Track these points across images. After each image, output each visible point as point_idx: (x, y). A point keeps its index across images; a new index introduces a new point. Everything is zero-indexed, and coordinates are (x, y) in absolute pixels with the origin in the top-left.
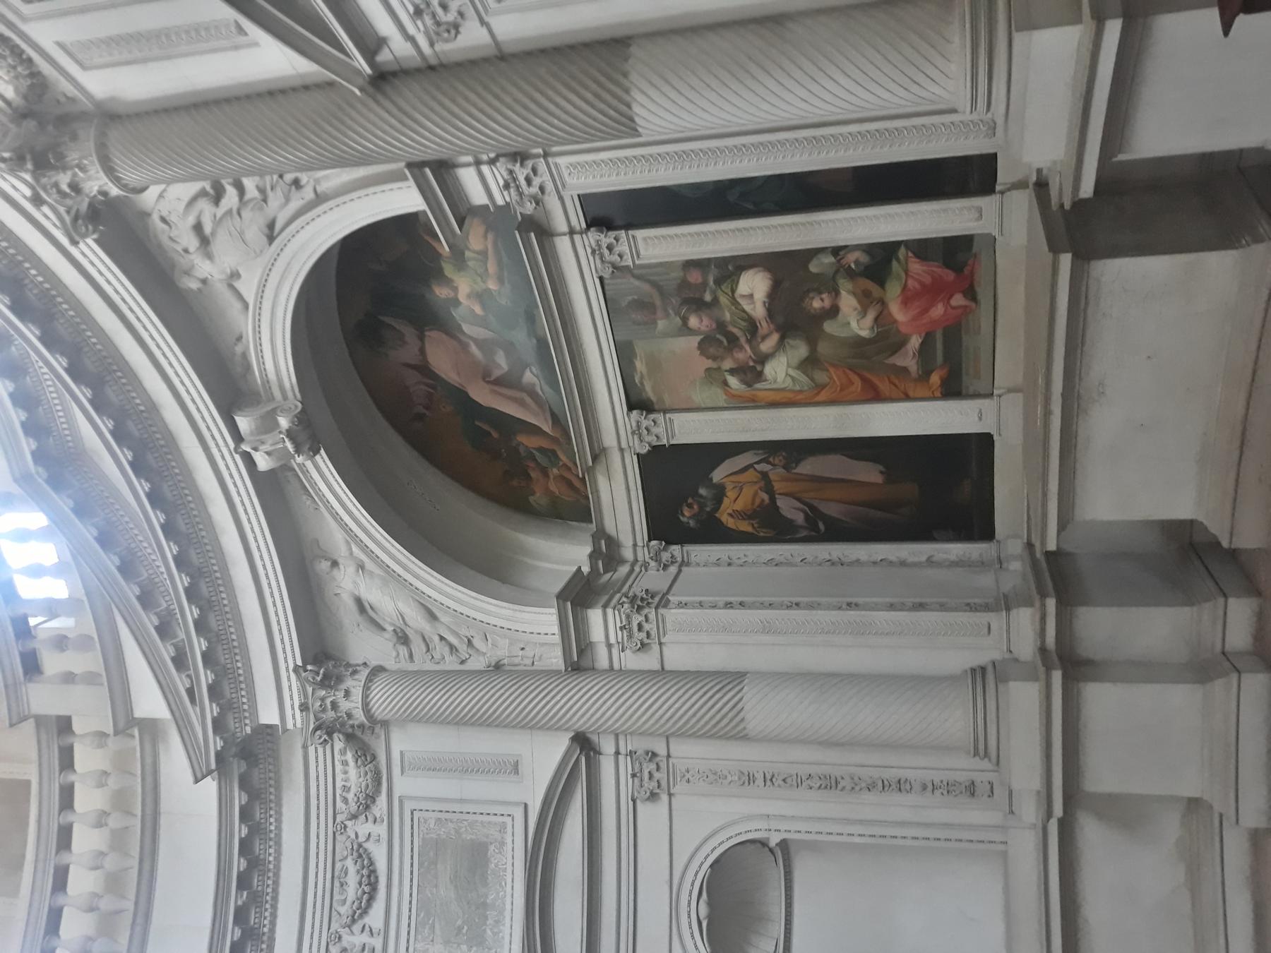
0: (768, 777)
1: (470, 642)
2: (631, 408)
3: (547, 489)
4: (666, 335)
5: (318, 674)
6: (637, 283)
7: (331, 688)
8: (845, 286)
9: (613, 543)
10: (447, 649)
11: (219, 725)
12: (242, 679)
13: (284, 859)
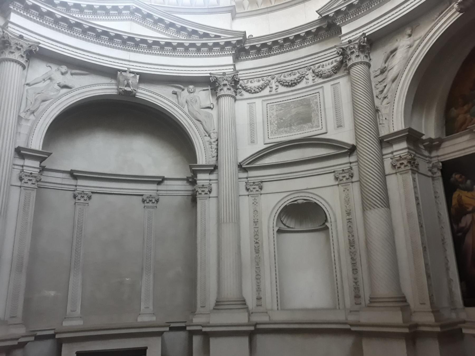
0: (350, 220)
1: (385, 98)
5: (363, 43)
7: (359, 50)
9: (438, 147)
10: (381, 89)
13: (296, 51)
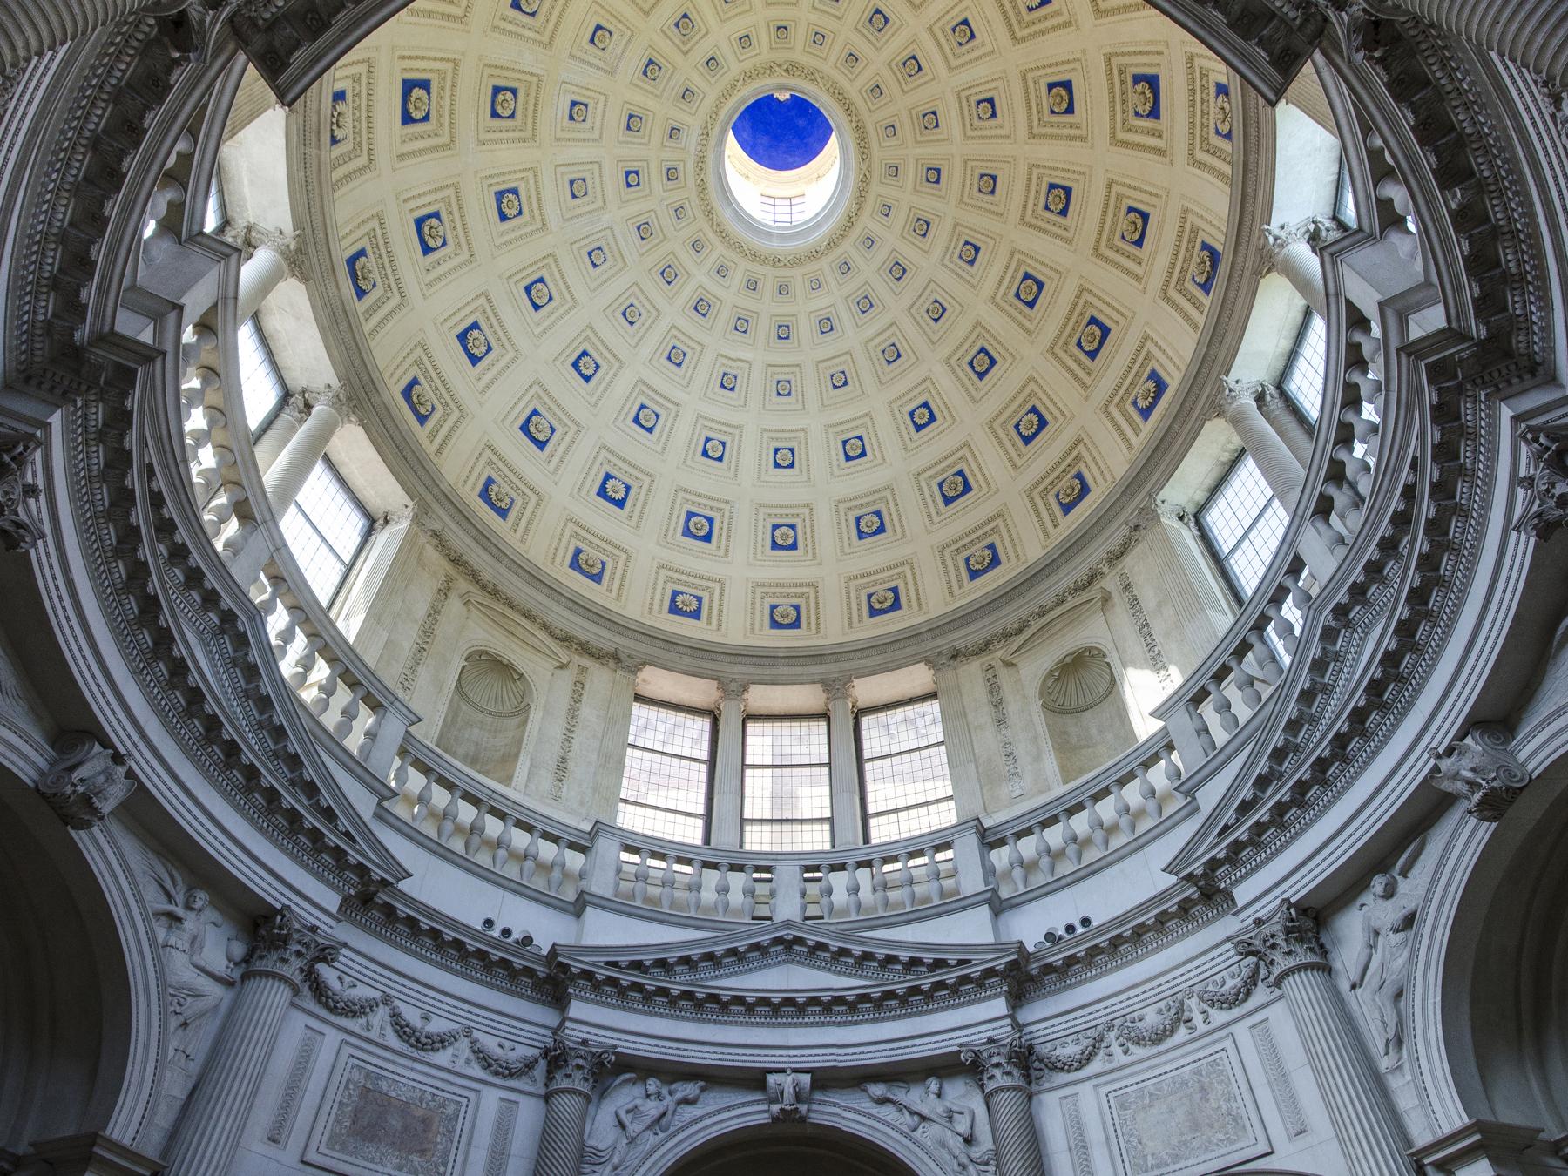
11: (587, 975)
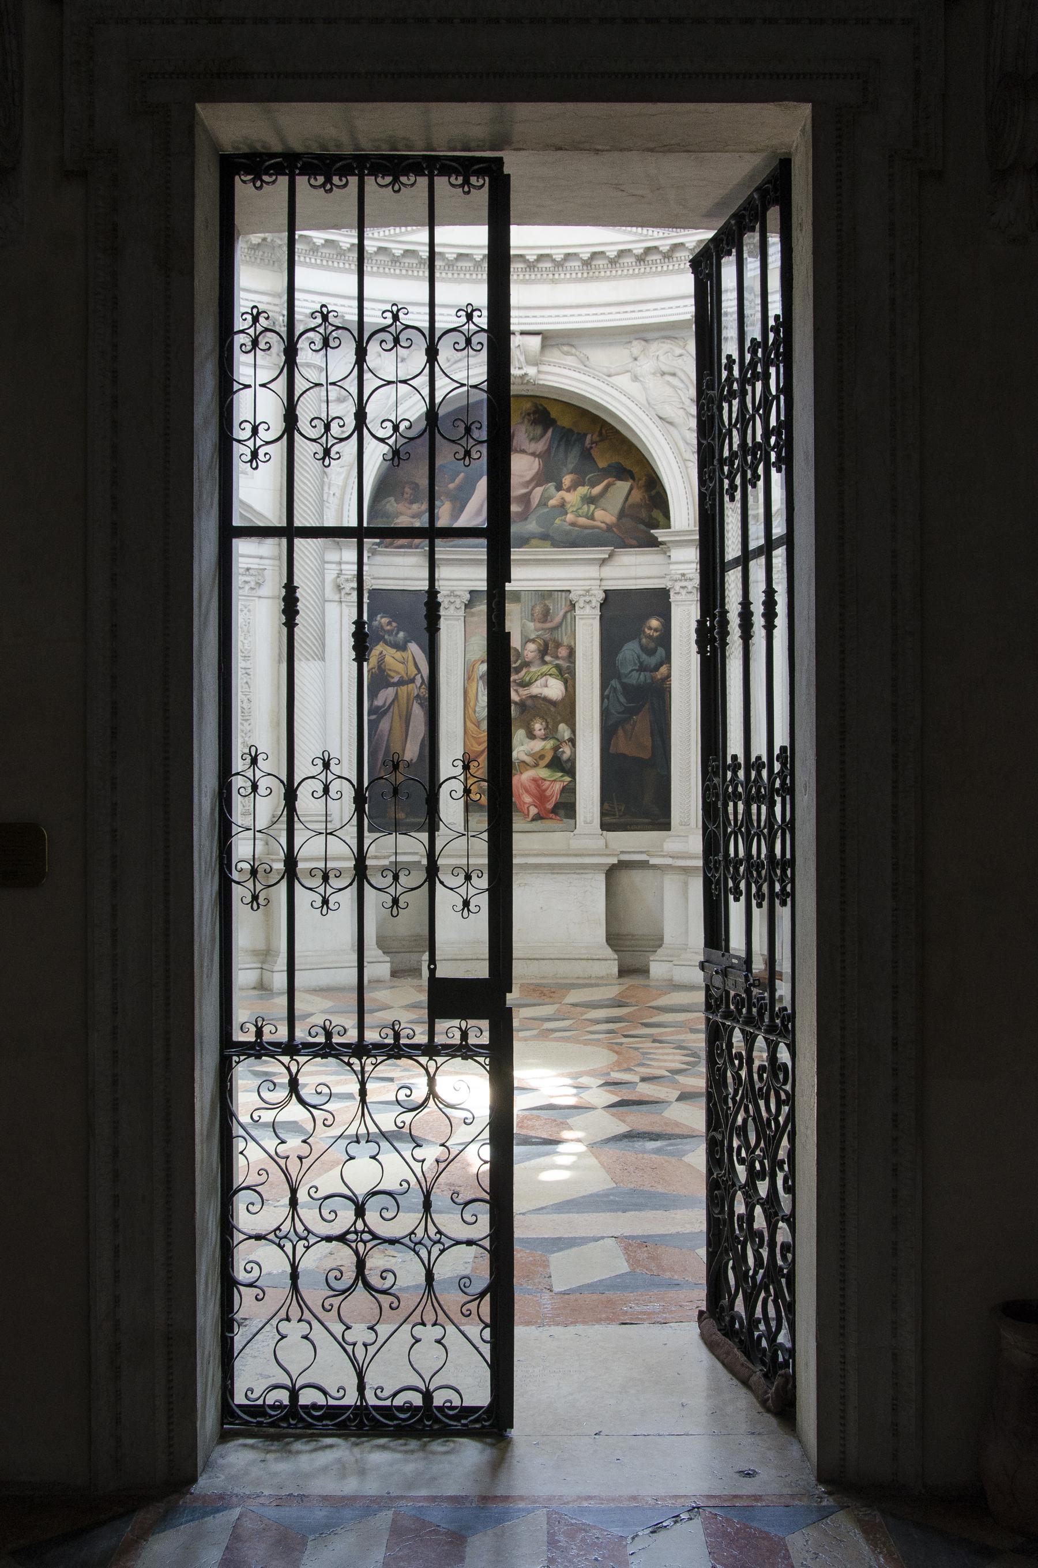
2: (471, 592)
3: (401, 514)
4: (523, 626)
6: (561, 613)
8: (550, 744)
12: (330, 263)
